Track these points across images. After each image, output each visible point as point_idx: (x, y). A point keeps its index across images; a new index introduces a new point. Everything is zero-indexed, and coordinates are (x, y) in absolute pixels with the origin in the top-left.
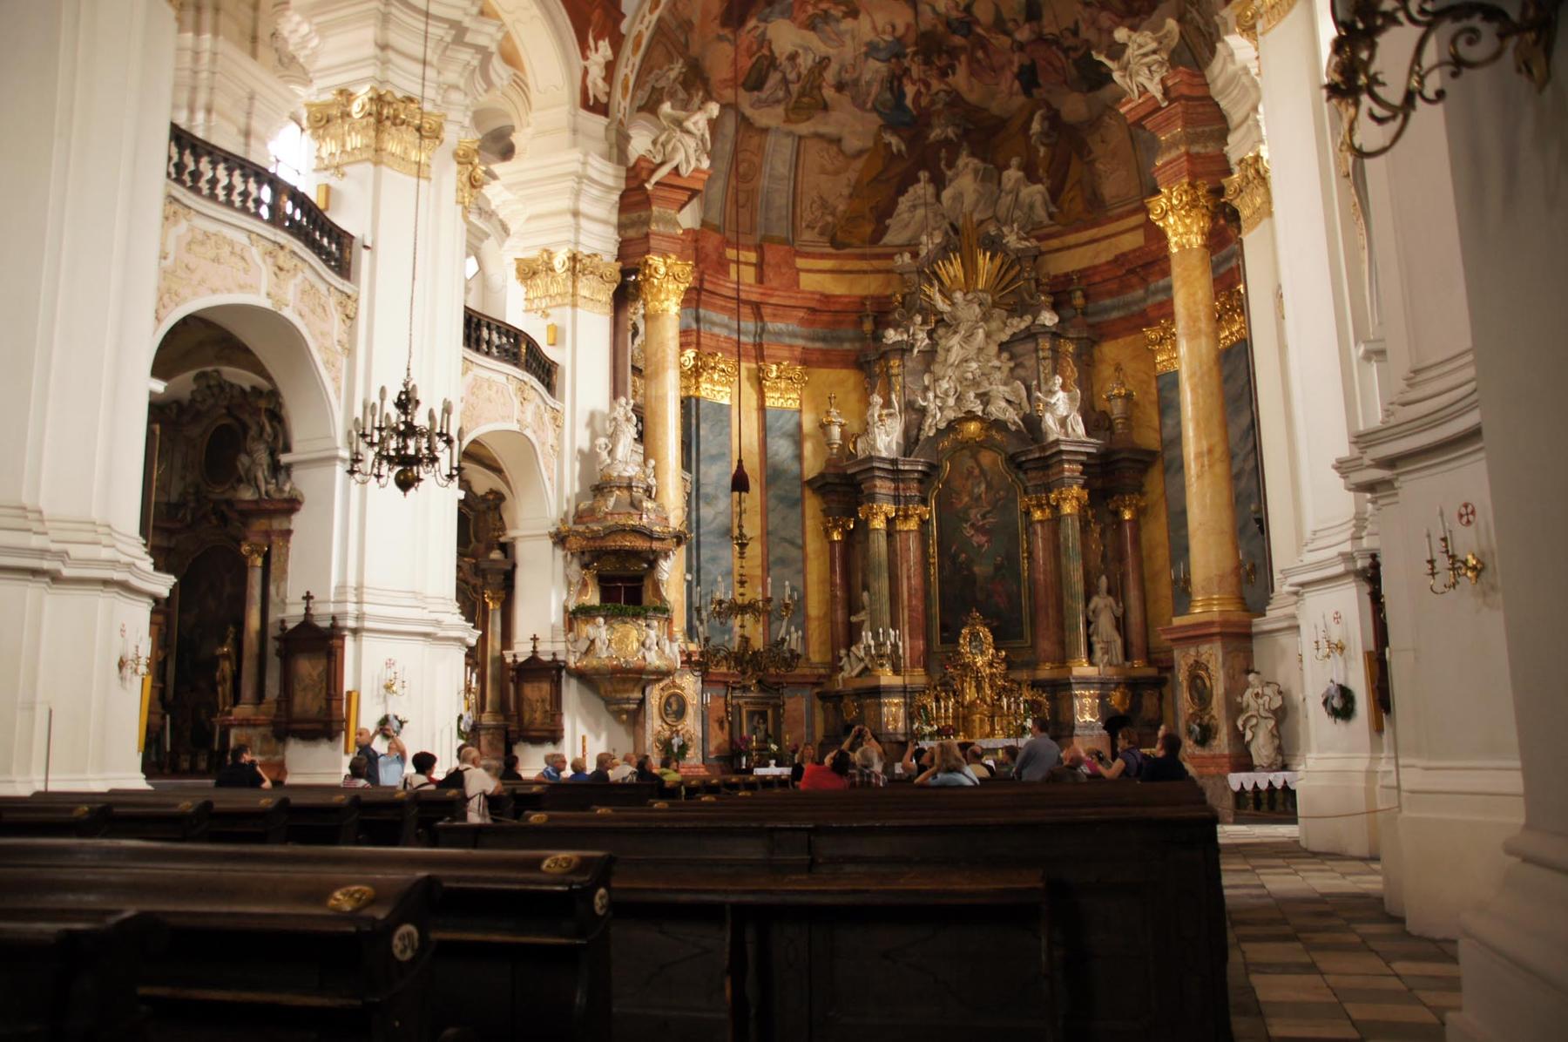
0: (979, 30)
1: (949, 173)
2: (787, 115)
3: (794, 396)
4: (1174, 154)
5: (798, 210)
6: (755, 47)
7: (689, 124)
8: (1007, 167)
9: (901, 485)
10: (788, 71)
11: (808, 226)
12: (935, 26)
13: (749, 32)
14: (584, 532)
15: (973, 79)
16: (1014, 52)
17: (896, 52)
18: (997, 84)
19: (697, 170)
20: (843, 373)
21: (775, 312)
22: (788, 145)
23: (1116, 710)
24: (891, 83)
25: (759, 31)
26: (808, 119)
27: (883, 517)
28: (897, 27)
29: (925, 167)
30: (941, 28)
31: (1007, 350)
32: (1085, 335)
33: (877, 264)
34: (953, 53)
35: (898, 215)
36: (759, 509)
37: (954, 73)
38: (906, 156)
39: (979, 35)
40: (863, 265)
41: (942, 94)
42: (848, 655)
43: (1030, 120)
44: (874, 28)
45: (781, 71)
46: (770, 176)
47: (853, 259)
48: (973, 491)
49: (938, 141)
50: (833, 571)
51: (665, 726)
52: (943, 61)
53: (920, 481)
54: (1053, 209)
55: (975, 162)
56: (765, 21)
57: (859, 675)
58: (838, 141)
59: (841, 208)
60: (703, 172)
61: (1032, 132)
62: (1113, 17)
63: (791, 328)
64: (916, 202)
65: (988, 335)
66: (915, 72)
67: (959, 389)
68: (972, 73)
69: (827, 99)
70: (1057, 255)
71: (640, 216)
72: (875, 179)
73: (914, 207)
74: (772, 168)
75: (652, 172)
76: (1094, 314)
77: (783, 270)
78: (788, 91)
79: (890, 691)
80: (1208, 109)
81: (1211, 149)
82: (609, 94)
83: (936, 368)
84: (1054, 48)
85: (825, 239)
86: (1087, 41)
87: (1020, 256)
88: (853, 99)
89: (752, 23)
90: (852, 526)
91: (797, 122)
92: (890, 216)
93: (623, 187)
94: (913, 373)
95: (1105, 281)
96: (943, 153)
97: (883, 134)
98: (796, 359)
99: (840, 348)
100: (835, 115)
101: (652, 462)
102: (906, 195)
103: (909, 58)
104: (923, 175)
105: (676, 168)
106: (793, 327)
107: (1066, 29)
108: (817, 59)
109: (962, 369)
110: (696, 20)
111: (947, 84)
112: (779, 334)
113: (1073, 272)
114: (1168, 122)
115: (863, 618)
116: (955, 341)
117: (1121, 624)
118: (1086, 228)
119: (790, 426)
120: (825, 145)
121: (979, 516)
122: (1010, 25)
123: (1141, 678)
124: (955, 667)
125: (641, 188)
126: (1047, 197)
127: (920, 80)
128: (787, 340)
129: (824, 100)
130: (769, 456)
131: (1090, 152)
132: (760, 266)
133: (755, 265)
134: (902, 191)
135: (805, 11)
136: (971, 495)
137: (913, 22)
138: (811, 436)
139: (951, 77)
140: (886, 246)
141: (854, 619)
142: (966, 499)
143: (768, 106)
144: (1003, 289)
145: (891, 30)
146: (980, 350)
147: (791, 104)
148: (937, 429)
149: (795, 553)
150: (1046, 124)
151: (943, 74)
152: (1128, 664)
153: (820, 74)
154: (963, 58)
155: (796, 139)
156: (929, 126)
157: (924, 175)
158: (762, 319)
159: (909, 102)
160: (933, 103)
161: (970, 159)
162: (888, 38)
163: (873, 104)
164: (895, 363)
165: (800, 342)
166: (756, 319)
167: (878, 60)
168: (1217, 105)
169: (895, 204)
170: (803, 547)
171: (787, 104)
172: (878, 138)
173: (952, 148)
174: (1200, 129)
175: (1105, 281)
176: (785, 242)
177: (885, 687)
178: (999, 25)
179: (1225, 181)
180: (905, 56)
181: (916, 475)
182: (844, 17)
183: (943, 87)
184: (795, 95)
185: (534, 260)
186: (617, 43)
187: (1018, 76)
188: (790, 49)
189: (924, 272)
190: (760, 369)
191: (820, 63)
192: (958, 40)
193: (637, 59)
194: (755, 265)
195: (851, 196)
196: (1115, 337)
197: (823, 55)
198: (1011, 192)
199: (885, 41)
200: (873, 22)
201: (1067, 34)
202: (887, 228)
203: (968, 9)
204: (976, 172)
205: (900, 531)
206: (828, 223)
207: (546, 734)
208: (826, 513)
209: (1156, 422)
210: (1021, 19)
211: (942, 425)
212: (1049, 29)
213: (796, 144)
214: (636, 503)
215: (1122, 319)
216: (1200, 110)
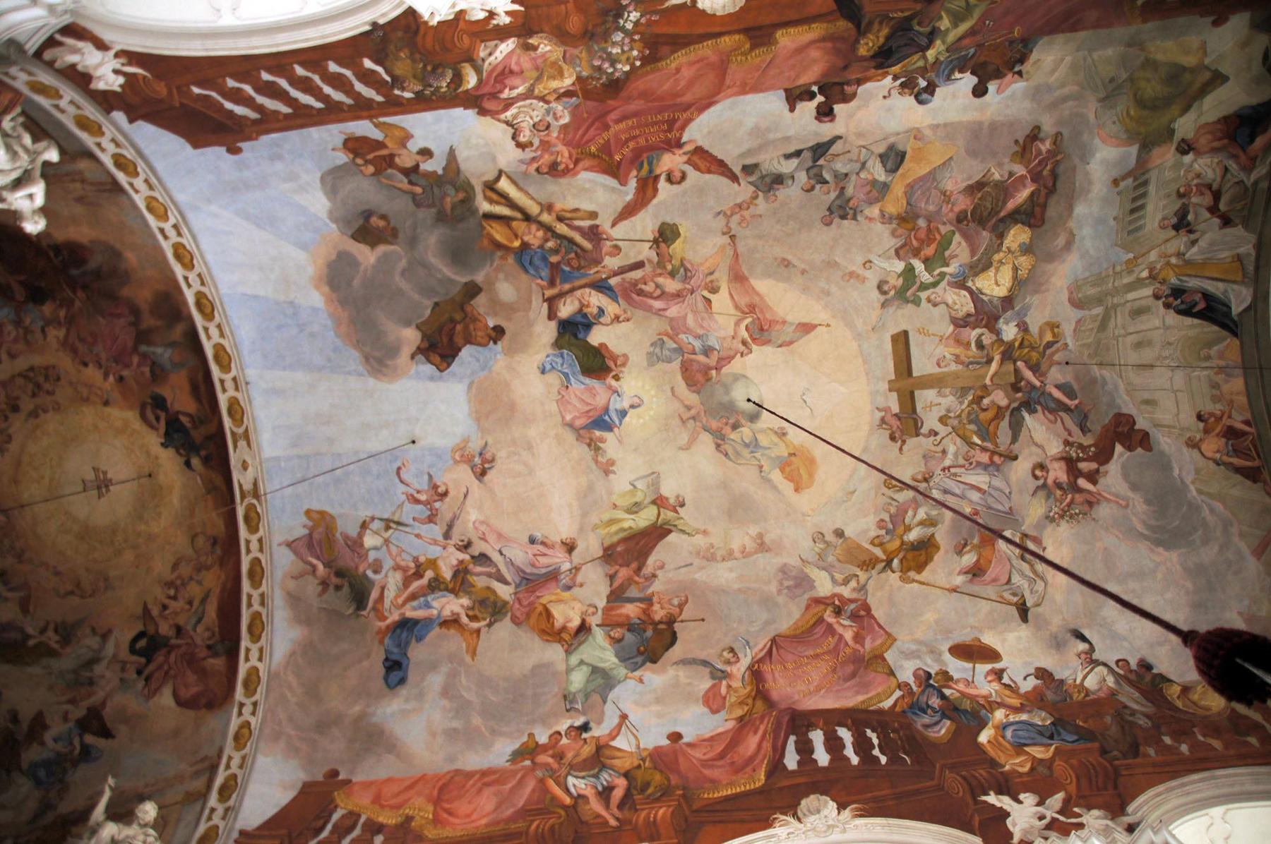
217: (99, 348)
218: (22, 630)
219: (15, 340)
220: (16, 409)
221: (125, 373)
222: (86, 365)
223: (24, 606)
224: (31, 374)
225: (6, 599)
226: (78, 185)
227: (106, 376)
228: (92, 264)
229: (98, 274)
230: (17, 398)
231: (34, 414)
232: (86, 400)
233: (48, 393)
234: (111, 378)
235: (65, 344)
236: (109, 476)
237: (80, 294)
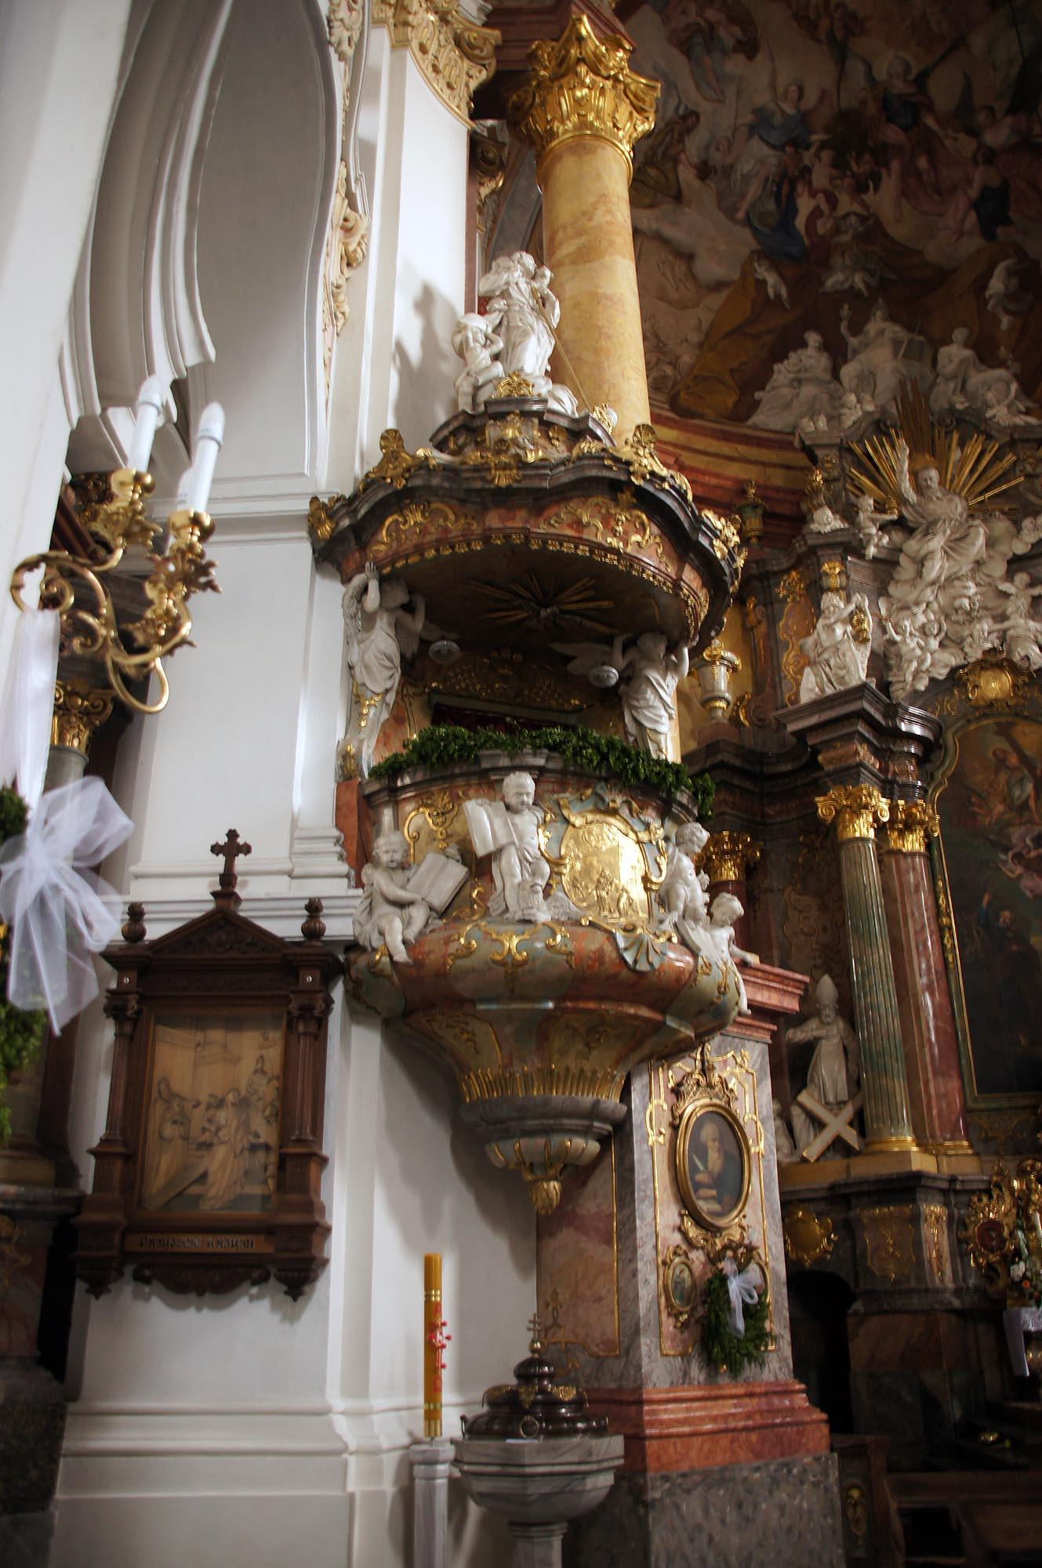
0: (930, 122)
1: (853, 342)
8: (948, 341)
12: (864, 103)
15: (904, 202)
16: (976, 163)
18: (941, 215)
24: (779, 185)
26: (652, 206)
30: (872, 109)
31: (1021, 570)
33: (742, 449)
34: (882, 154)
35: (774, 388)
37: (876, 188)
38: (787, 306)
39: (927, 128)
40: (726, 448)
41: (853, 219)
43: (988, 275)
44: (773, 86)
47: (706, 435)
48: (1011, 797)
49: (837, 292)
51: (693, 1232)
52: (860, 167)
55: (894, 330)
58: (689, 257)
59: (687, 359)
61: (987, 294)
64: (802, 375)
65: (990, 543)
66: (820, 176)
67: (945, 627)
68: (905, 193)
69: (682, 184)
72: (735, 331)
73: (798, 382)
83: (892, 589)
88: (720, 197)
92: (763, 388)
96: (845, 311)
97: (756, 265)
102: (786, 362)
103: (813, 150)
104: (813, 338)
108: (681, 112)
109: (952, 591)
115: (816, 1033)
116: (937, 543)
120: (670, 258)
121: (1028, 841)
129: (678, 181)
134: (782, 357)
135: (684, 13)
136: (1007, 799)
139: (871, 191)
140: (755, 427)
142: (1000, 808)
144: (986, 490)
145: (795, 95)
146: (978, 563)
148: (932, 680)
150: (1014, 281)
151: (860, 188)
153: (681, 140)
154: (895, 165)
156: (826, 266)
157: (813, 338)
159: (800, 222)
160: (837, 231)
161: (887, 325)
162: (790, 110)
163: (747, 214)
167: (768, 144)
169: (770, 372)
172: (747, 271)
173: (861, 306)
178: (964, 117)
180: (807, 147)
182: (734, 51)
183: (856, 208)
187: (976, 205)
189: (850, 451)
191: (684, 118)
192: (893, 134)
195: (701, 345)
197: (691, 107)
198: (955, 377)
199: (784, 113)
200: (774, 75)
202: (755, 405)
204: (896, 344)
206: (665, 377)
207: (259, 1245)
211: (941, 673)
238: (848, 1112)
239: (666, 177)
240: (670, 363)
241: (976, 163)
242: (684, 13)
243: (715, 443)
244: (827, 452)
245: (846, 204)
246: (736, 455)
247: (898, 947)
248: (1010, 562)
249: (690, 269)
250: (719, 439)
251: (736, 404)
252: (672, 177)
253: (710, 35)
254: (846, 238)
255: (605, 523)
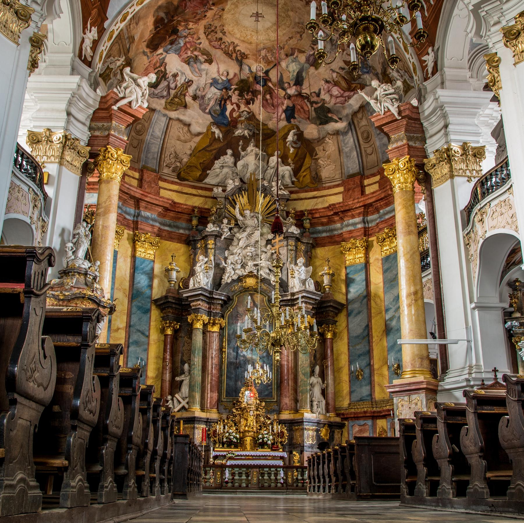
0: (270, 84)
1: (243, 153)
2: (166, 105)
3: (152, 252)
4: (400, 144)
5: (163, 156)
6: (158, 65)
7: (140, 81)
8: (273, 155)
9: (212, 307)
10: (171, 82)
11: (166, 166)
12: (249, 78)
13: (158, 55)
14: (58, 296)
16: (285, 99)
17: (226, 87)
18: (274, 113)
19: (140, 107)
20: (179, 245)
21: (147, 206)
22: (163, 121)
23: (323, 439)
24: (221, 101)
25: (163, 56)
26: (176, 110)
27: (202, 322)
28: (230, 74)
29: (231, 148)
30: (251, 79)
32: (311, 242)
33: (200, 192)
34: (255, 93)
36: (126, 311)
37: (253, 104)
39: (269, 87)
40: (194, 191)
41: (245, 113)
42: (172, 400)
43: (287, 134)
44: (218, 72)
45: (168, 81)
46: (152, 135)
47: (188, 187)
49: (239, 136)
50: (165, 351)
52: (249, 97)
53: (222, 306)
54: (294, 179)
56: (167, 52)
57: (179, 411)
58: (189, 125)
59: (185, 160)
60: (143, 109)
61: (287, 140)
62: (340, 90)
63: (153, 216)
64: (224, 165)
65: (262, 235)
67: (243, 261)
70: (295, 202)
71: (103, 125)
72: (203, 149)
73: (223, 167)
74: (153, 131)
75: (117, 101)
76: (313, 233)
77: (153, 185)
78: (169, 92)
79: (199, 420)
80: (417, 126)
81: (418, 145)
82: (92, 57)
83: (230, 248)
84: (306, 101)
85: (175, 174)
86: (324, 100)
87: (280, 198)
88: (200, 105)
89: (160, 51)
90: (178, 327)
91: (169, 110)
92: (210, 169)
93: (98, 107)
94: (220, 249)
95: (321, 217)
96: (241, 143)
98: (154, 233)
99: (177, 232)
100: (189, 112)
101: (98, 263)
103: (232, 91)
104: (229, 152)
105: (130, 103)
106: (155, 216)
107: (314, 92)
108: (186, 81)
110: (136, 38)
111: (249, 108)
112: (147, 218)
113: (305, 210)
114: (398, 128)
117: (324, 393)
118: (311, 191)
119: (148, 268)
120: (182, 126)
122: (286, 85)
123: (335, 423)
124: (237, 409)
125: (109, 109)
126: (292, 173)
127: (236, 103)
128: (151, 222)
130: (135, 283)
131: (316, 154)
132: (141, 180)
133: (138, 179)
137: (238, 72)
138: (158, 276)
140: (206, 184)
141: (178, 379)
143: (157, 98)
145: (226, 74)
147: (169, 101)
149: (143, 339)
150: (296, 137)
151: (248, 103)
152: (328, 415)
153: (187, 89)
155: (168, 119)
156: (235, 127)
157: (229, 152)
158: (139, 208)
159: (228, 113)
160: (240, 116)
162: (224, 79)
163: (210, 110)
164: (211, 242)
165: (157, 224)
166: (135, 207)
167: (217, 88)
168: (422, 124)
169: (213, 164)
170: (148, 337)
171: (167, 99)
173: (246, 141)
174: (412, 135)
175: (321, 217)
176: (154, 171)
177: (198, 418)
178: (281, 84)
179: (425, 160)
180: (230, 90)
181: (220, 302)
182: (204, 62)
183: (246, 109)
184: (172, 96)
185: (40, 134)
186: (101, 31)
187: (285, 111)
188: (174, 71)
189: (228, 199)
190: (135, 235)
191: (188, 82)
193: (109, 44)
194: (138, 179)
195: (191, 155)
196: (323, 245)
198: (274, 168)
199: (222, 79)
200: (218, 68)
201: (313, 94)
203: (267, 72)
205: (210, 331)
206: (177, 167)
208: (164, 319)
209: (344, 290)
210: (292, 83)
212: (305, 91)
213: (168, 121)
214: (88, 284)
215: (328, 237)
216: (414, 125)
217: (199, 12)
218: (310, 55)
219: (193, 38)
220: (221, 39)
221: (211, 3)
222: (206, 16)
223: (301, 52)
224: (207, 33)
225: (297, 57)
226: (131, 26)
227: (212, 9)
228: (162, 14)
229: (167, 14)
230: (216, 38)
231: (224, 33)
232: (220, 16)
233: (216, 27)
234: (213, 7)
235: (196, 22)
236: (255, 12)
237: (175, 18)
238: (187, 400)
239: (181, 101)
240: (179, 162)
241: (285, 99)
242: (186, 53)
243: (191, 189)
244: (221, 199)
245: (243, 107)
246: (197, 194)
247: (205, 358)
248: (267, 241)
249: (189, 130)
250: (192, 188)
251: (200, 175)
252: (183, 100)
253: (196, 58)
254: (243, 119)
255: (82, 303)
